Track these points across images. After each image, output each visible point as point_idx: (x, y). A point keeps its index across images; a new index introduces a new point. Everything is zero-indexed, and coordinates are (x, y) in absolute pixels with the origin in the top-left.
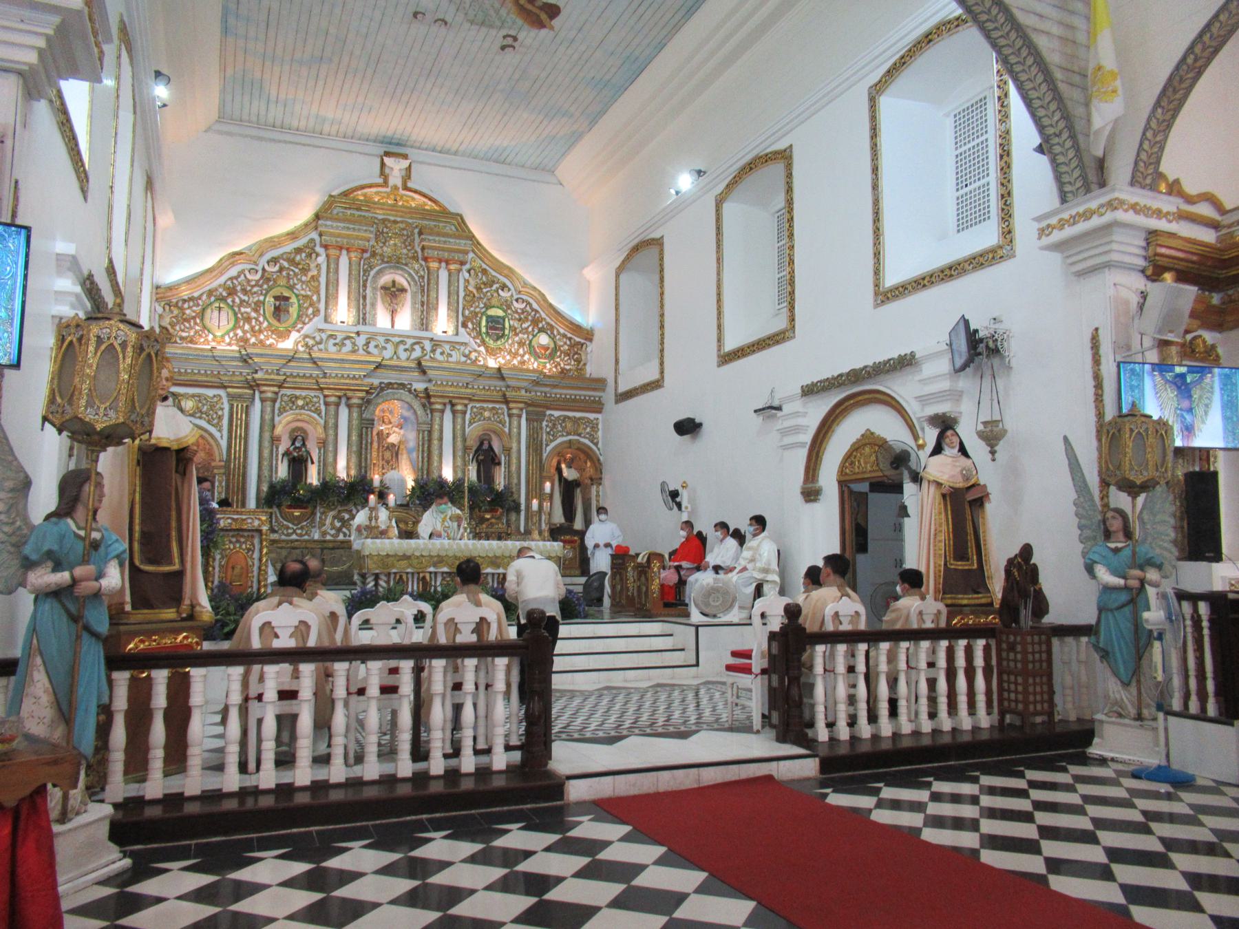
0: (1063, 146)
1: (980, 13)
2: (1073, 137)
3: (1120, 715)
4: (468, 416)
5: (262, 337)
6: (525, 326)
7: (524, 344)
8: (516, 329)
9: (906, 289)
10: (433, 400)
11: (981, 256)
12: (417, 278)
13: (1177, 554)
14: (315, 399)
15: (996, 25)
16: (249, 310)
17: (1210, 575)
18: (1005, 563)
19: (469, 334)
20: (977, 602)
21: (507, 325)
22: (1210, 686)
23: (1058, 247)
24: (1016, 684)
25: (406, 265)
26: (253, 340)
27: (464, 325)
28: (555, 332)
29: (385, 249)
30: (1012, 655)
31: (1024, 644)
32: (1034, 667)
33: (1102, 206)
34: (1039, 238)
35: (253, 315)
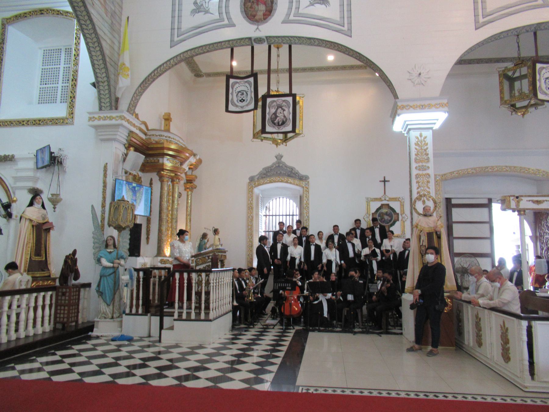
0: (104, 87)
1: (82, 20)
2: (109, 85)
3: (105, 318)
9: (12, 123)
11: (57, 120)
13: (129, 254)
15: (87, 28)
17: (136, 262)
18: (64, 257)
20: (43, 275)
22: (141, 302)
23: (96, 127)
24: (64, 310)
30: (63, 298)
31: (70, 292)
32: (65, 302)
33: (117, 117)
34: (89, 121)
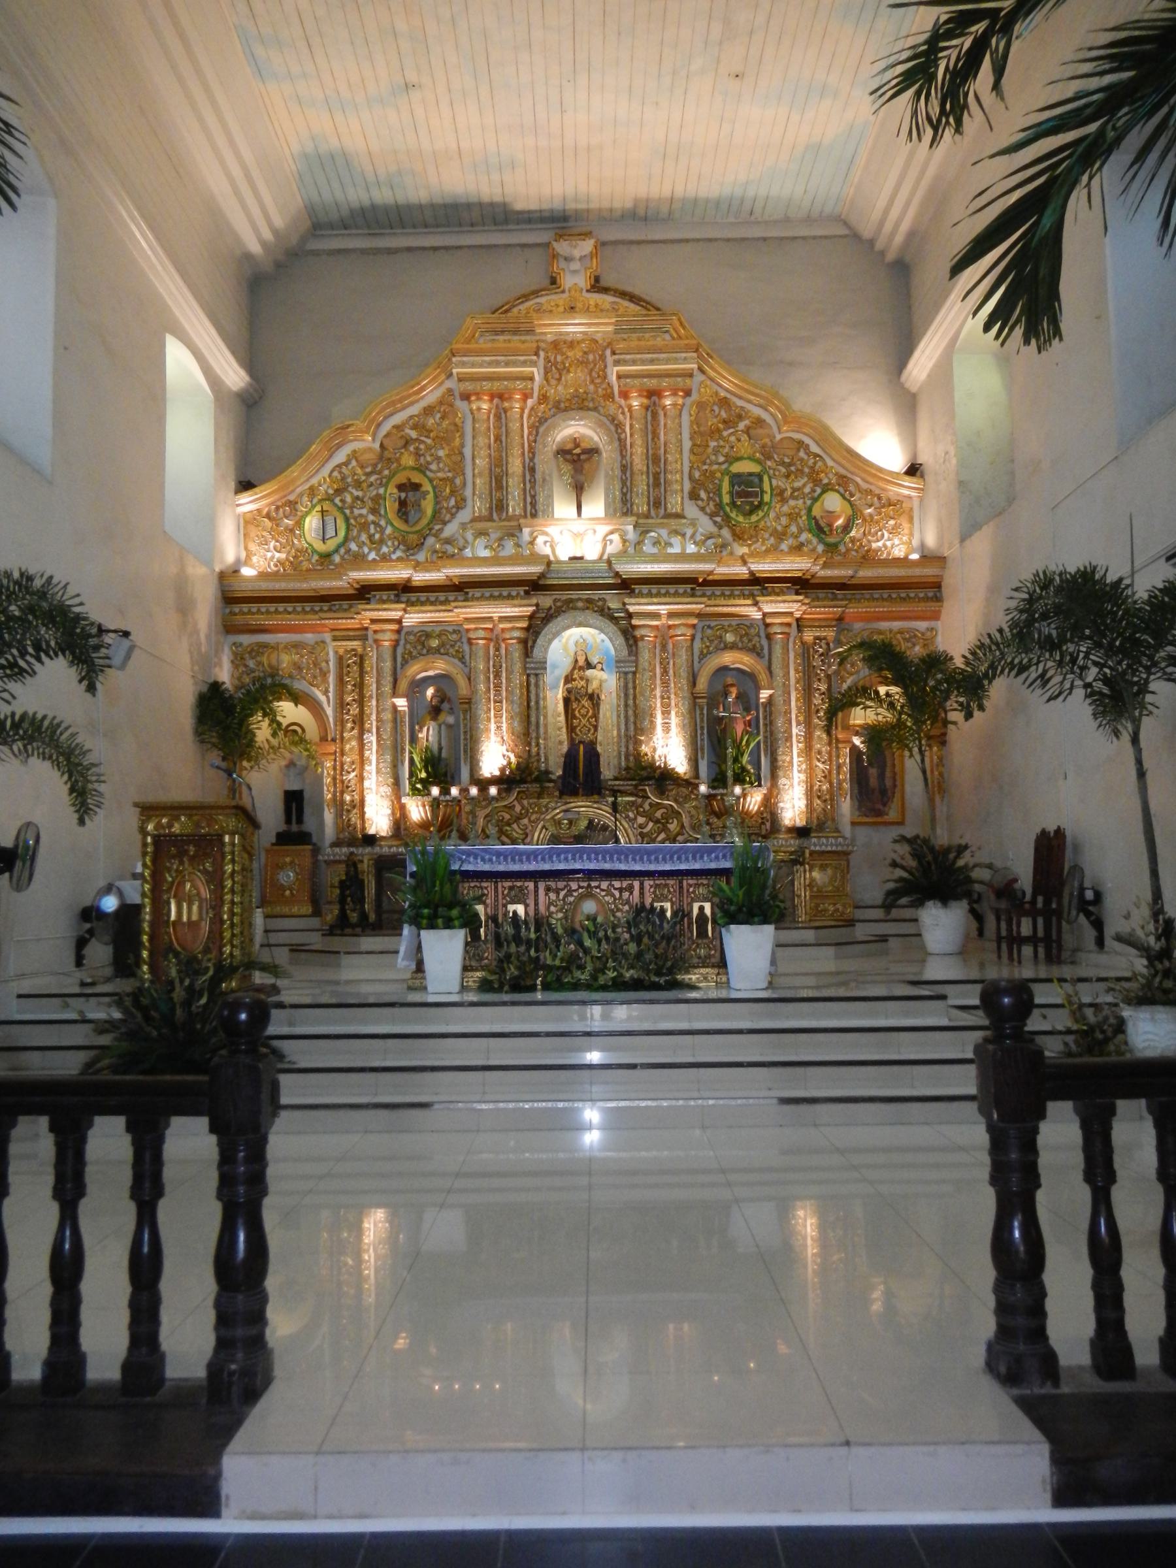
4: (697, 645)
5: (385, 549)
6: (797, 484)
7: (798, 515)
8: (782, 492)
10: (635, 622)
12: (613, 428)
14: (455, 637)
16: (364, 511)
19: (702, 509)
21: (766, 486)
25: (595, 409)
26: (372, 556)
27: (694, 496)
28: (852, 488)
29: (560, 388)
35: (371, 518)
